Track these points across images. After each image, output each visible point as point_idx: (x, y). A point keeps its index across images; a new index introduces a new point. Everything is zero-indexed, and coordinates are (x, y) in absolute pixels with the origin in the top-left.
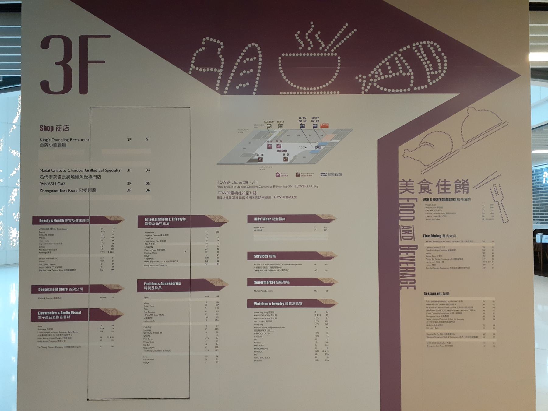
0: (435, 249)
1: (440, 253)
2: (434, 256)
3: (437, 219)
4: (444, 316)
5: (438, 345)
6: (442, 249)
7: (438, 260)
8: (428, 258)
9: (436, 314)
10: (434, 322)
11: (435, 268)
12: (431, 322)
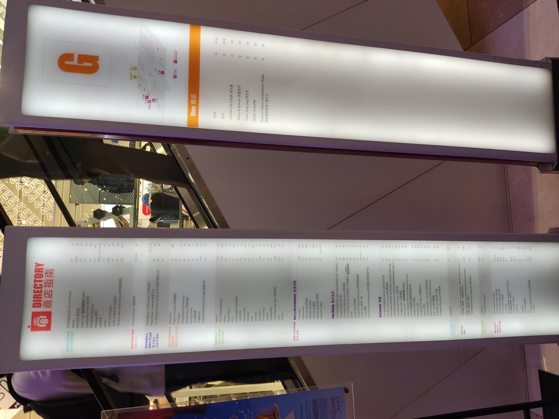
3: (321, 305)
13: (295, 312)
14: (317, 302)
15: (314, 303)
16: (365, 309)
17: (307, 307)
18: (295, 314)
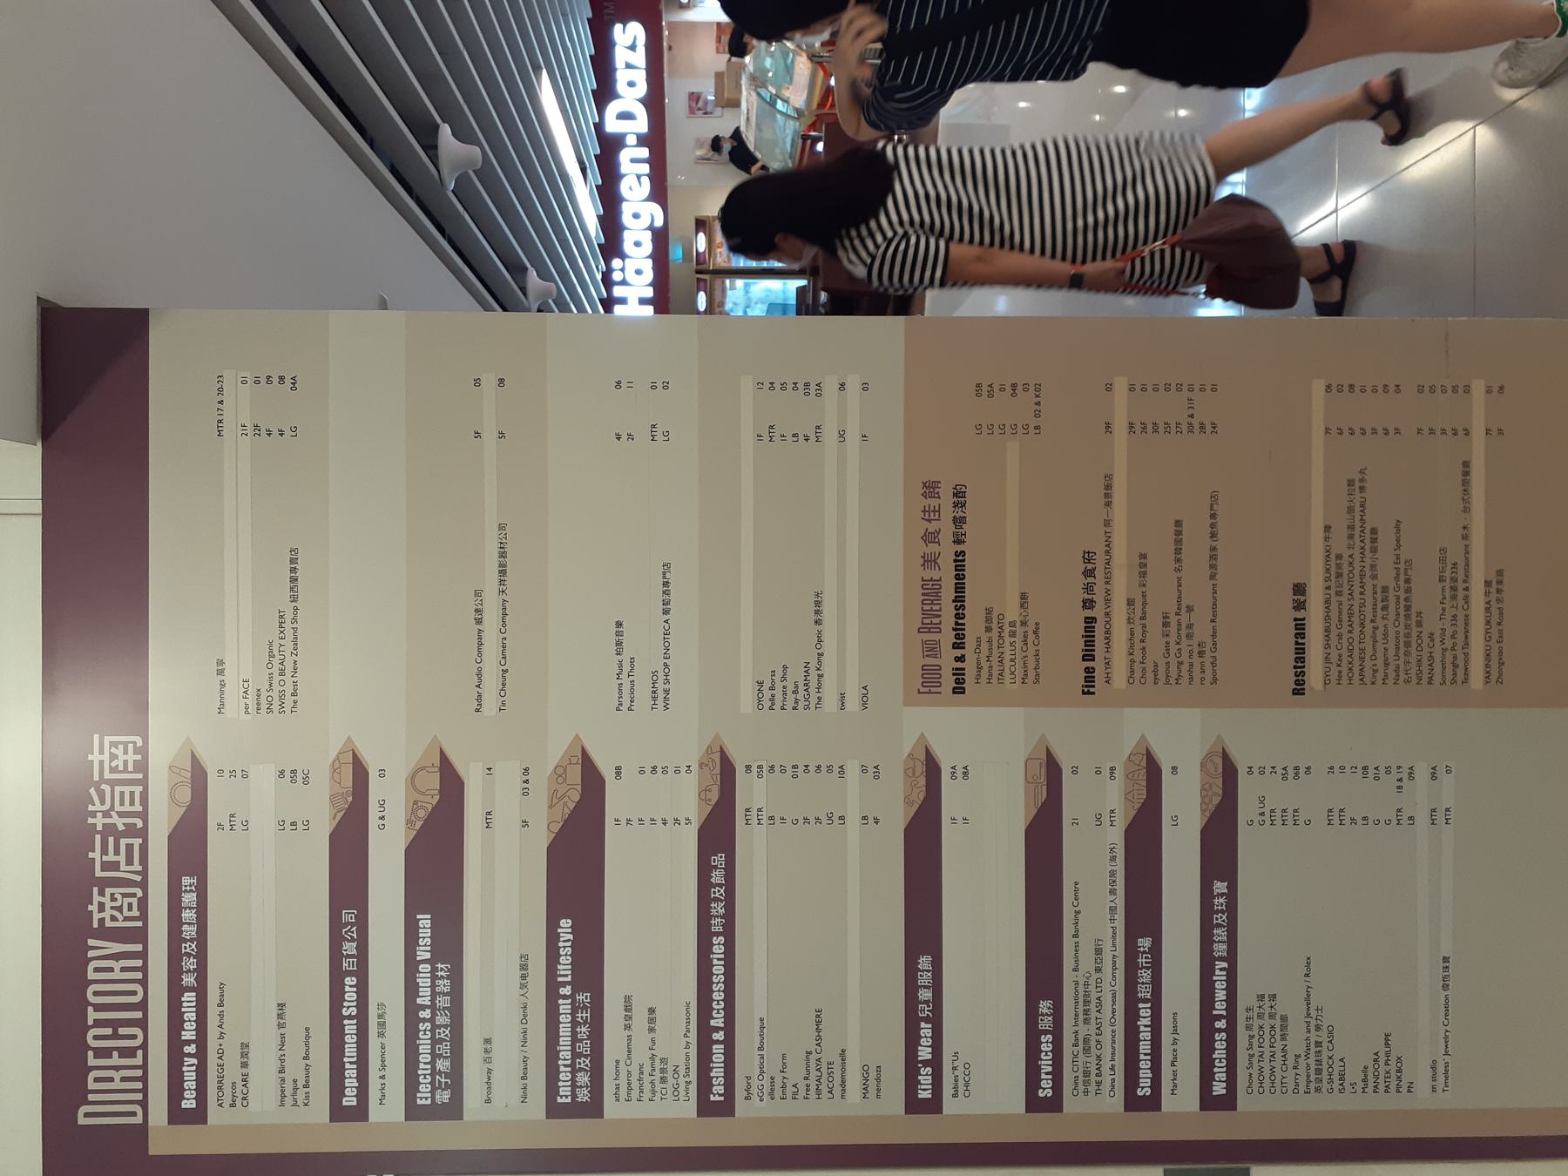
0: (1138, 646)
1: (1155, 623)
2: (1168, 650)
4: (1385, 608)
5: (1495, 636)
6: (1139, 614)
7: (1183, 633)
8: (1174, 673)
9: (1375, 641)
10: (1407, 654)
11: (1215, 644)
12: (1407, 662)
13: (959, 653)
14: (1024, 623)
15: (1012, 624)
16: (1201, 654)
17: (990, 641)
18: (960, 665)
